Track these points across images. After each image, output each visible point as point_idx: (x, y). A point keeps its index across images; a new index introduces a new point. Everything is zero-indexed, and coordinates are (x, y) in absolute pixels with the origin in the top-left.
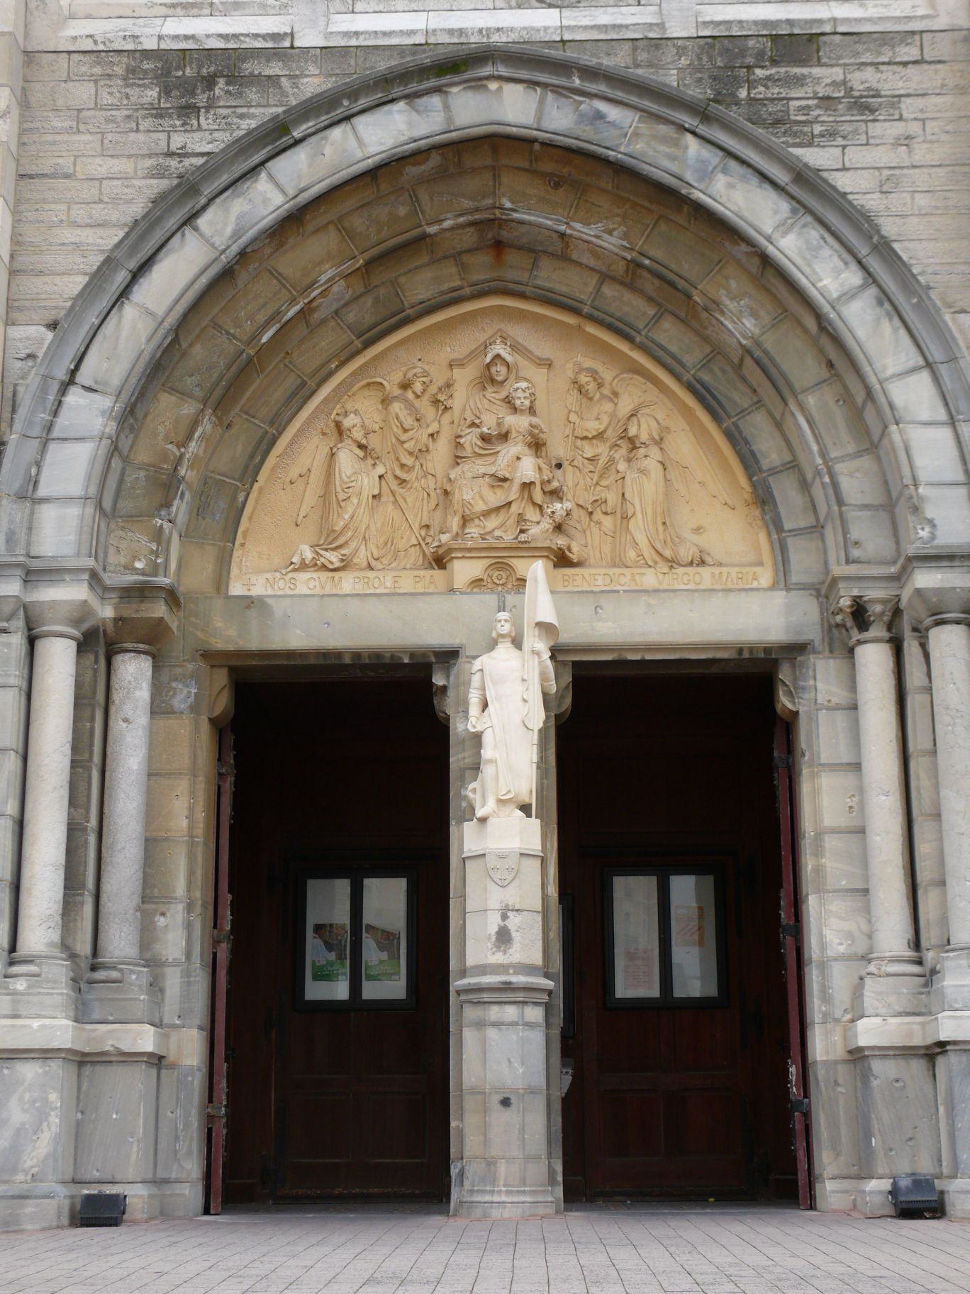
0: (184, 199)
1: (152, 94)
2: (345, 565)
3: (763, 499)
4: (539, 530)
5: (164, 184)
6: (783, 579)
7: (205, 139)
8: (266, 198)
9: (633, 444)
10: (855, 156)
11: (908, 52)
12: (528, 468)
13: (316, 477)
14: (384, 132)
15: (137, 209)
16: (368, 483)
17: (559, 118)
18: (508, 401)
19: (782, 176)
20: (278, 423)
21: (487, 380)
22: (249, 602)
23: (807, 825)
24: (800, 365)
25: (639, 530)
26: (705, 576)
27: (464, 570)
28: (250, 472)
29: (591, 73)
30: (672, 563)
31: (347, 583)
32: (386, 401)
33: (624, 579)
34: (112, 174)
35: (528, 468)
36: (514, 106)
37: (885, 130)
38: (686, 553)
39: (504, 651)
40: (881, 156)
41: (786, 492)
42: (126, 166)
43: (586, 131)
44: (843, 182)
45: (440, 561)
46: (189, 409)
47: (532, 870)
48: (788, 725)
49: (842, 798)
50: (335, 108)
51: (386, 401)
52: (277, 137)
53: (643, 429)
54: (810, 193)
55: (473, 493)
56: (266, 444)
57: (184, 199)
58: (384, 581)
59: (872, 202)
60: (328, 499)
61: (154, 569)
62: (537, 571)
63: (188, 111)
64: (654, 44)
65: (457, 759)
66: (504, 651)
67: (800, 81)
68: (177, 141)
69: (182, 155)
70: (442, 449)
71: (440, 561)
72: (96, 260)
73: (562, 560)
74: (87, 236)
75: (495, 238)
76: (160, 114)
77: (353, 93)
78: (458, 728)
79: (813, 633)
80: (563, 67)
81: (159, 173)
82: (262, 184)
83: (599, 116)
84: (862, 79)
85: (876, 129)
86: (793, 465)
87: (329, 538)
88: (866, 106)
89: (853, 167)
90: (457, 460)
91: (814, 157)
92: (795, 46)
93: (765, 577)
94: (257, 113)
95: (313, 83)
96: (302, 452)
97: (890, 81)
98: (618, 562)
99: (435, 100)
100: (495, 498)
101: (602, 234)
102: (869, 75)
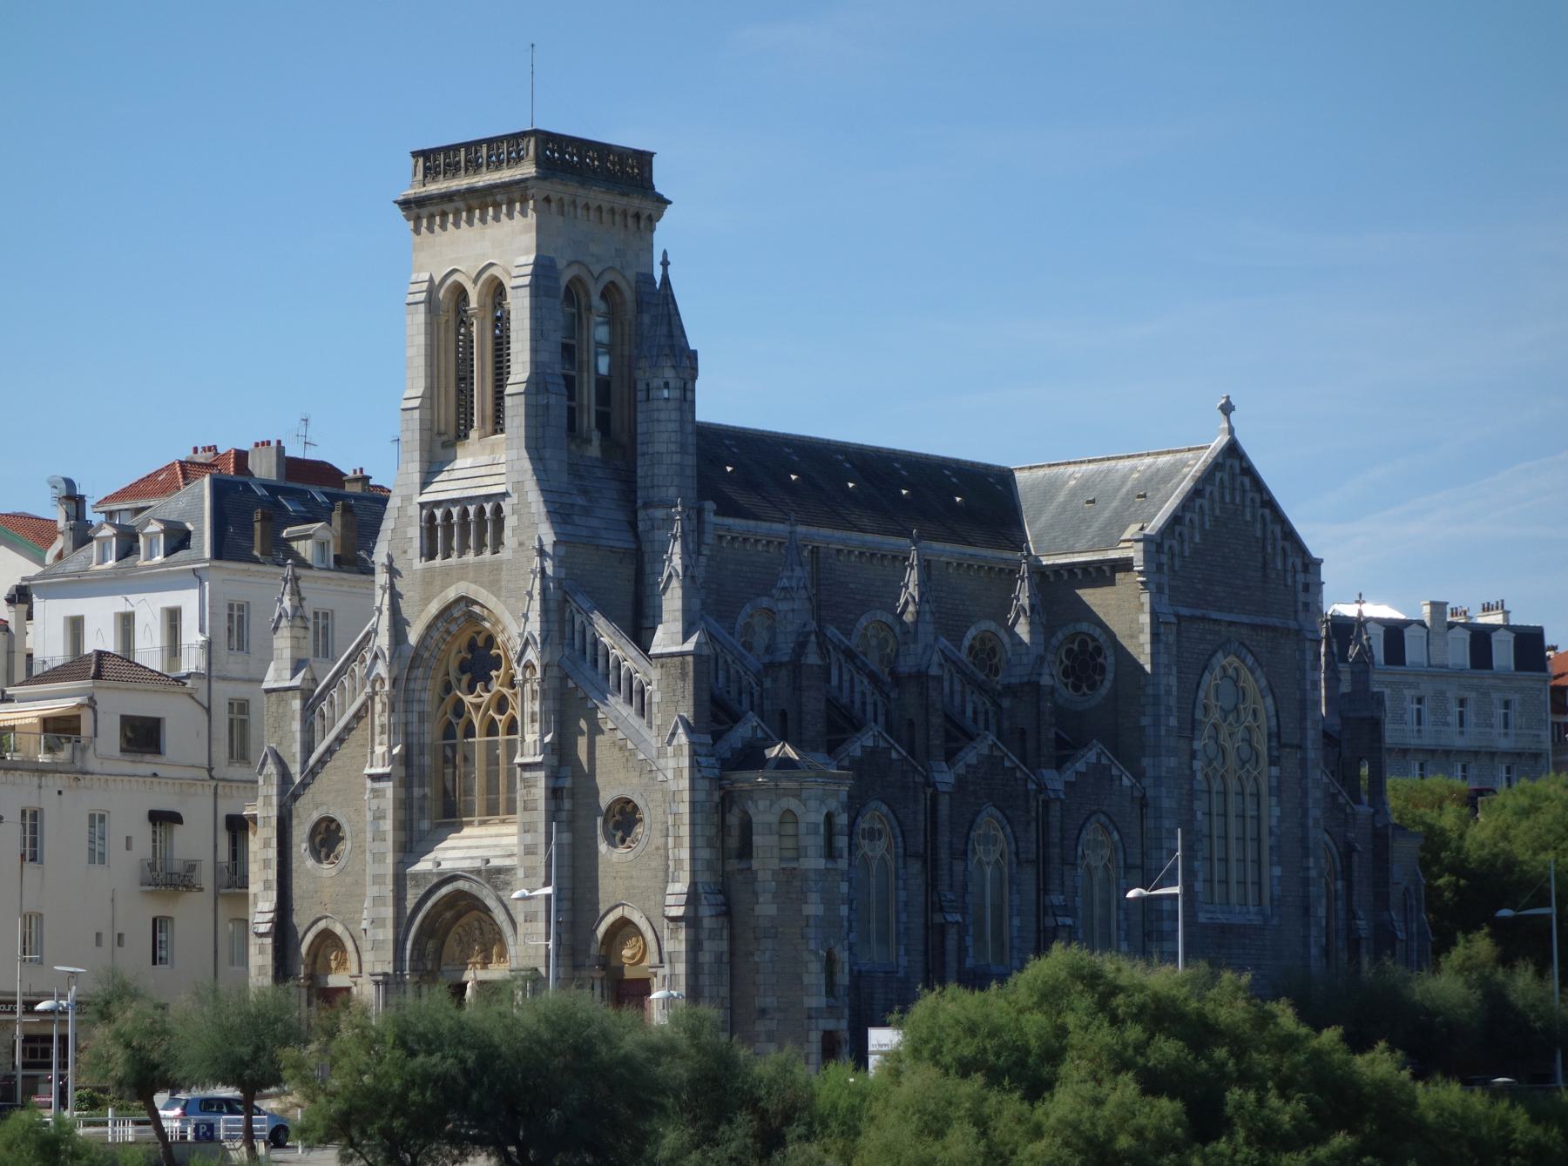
95: (435, 880)
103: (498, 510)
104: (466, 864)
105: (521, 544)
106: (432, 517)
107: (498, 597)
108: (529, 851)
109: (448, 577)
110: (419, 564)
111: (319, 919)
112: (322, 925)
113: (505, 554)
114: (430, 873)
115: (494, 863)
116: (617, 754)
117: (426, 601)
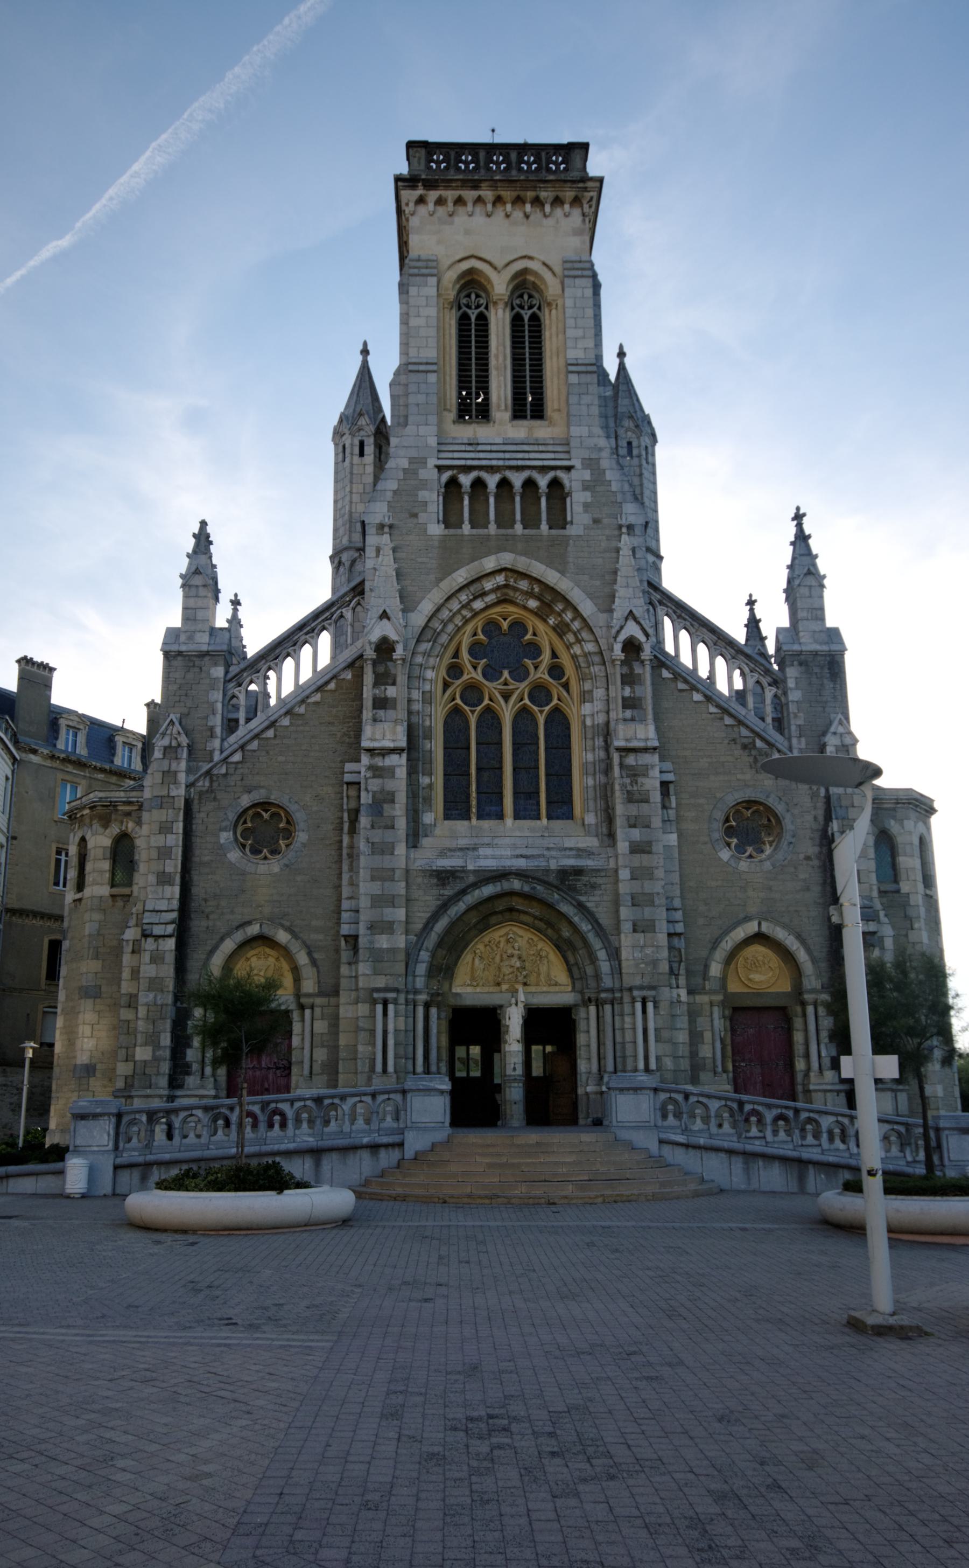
0: (444, 907)
1: (435, 881)
2: (477, 985)
3: (570, 971)
4: (520, 978)
5: (439, 903)
6: (574, 990)
7: (448, 892)
8: (461, 906)
9: (541, 957)
10: (591, 898)
11: (603, 874)
12: (518, 964)
13: (470, 965)
14: (488, 890)
15: (433, 908)
16: (482, 966)
17: (527, 888)
18: (513, 947)
19: (574, 902)
20: (462, 952)
21: (508, 941)
22: (457, 994)
23: (578, 1045)
24: (579, 944)
25: (542, 978)
26: (557, 989)
27: (504, 987)
28: (456, 964)
29: (533, 878)
30: (550, 985)
31: (478, 990)
32: (486, 946)
33: (539, 989)
34: (427, 900)
35: (518, 964)
36: (516, 884)
37: (598, 892)
38: (553, 982)
39: (514, 1006)
40: (597, 899)
41: (575, 970)
42: (430, 898)
43: (532, 891)
44: (588, 905)
45: (499, 984)
46: (444, 952)
47: (520, 1054)
48: (574, 1021)
49: (586, 1038)
50: (475, 885)
51: (486, 946)
52: (463, 892)
53: (544, 954)
54: (581, 907)
55: (506, 970)
56: (459, 957)
57: (444, 907)
58: (486, 989)
59: (594, 909)
60: (473, 969)
61: (438, 989)
62: (520, 988)
63: (444, 885)
64: (547, 871)
65: (503, 1029)
66: (514, 1006)
67: (579, 880)
68: (442, 892)
69: (443, 895)
70: (498, 959)
71: (499, 984)
72: (424, 921)
73: (525, 984)
74: (422, 915)
75: (511, 910)
76: (438, 885)
77: (481, 882)
78: (503, 1022)
79: (580, 1002)
80: (527, 877)
81: (439, 900)
82: (461, 903)
83: (535, 888)
84: (593, 880)
85: (596, 892)
86: (577, 964)
87: (473, 978)
88: (594, 886)
89: (590, 902)
90: (502, 960)
91: (583, 899)
92: (578, 872)
93: (570, 989)
94: (459, 886)
95: (472, 879)
96: (467, 957)
97: (599, 881)
98: (537, 985)
99: (499, 884)
100: (511, 970)
101: (535, 910)
102: (594, 879)
103: (555, 484)
104: (521, 863)
105: (596, 521)
106: (453, 483)
107: (563, 573)
108: (638, 849)
109: (483, 547)
110: (436, 530)
111: (249, 923)
112: (254, 930)
113: (571, 530)
114: (464, 870)
115: (571, 862)
116: (738, 751)
117: (446, 571)
